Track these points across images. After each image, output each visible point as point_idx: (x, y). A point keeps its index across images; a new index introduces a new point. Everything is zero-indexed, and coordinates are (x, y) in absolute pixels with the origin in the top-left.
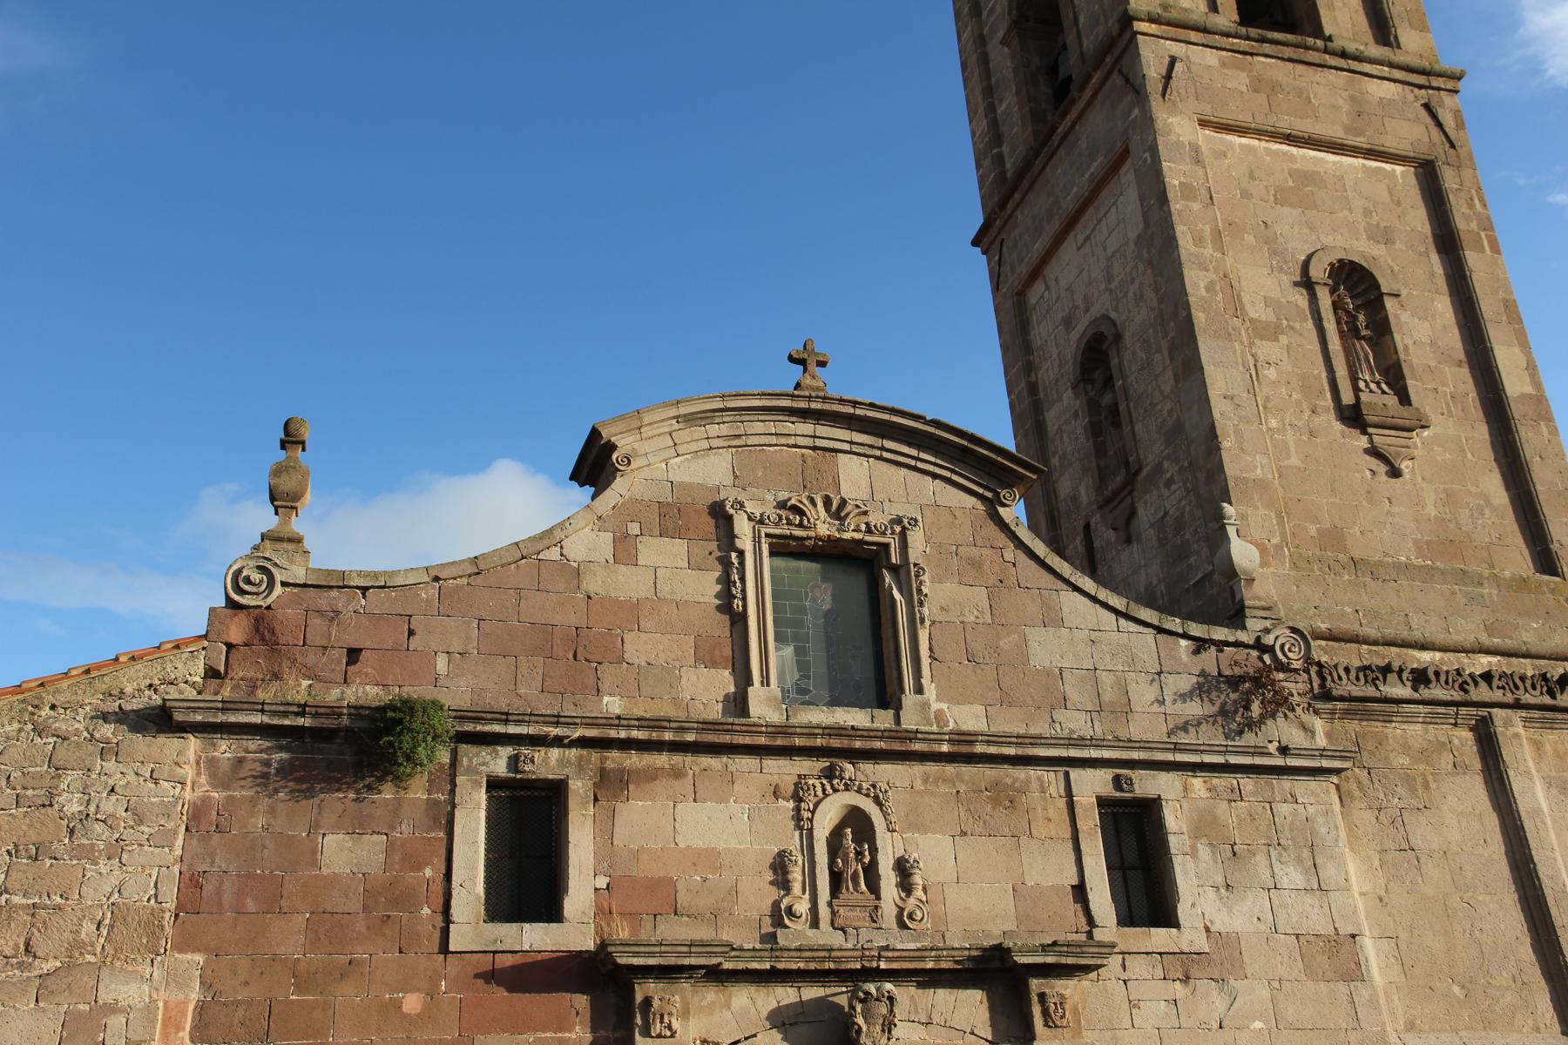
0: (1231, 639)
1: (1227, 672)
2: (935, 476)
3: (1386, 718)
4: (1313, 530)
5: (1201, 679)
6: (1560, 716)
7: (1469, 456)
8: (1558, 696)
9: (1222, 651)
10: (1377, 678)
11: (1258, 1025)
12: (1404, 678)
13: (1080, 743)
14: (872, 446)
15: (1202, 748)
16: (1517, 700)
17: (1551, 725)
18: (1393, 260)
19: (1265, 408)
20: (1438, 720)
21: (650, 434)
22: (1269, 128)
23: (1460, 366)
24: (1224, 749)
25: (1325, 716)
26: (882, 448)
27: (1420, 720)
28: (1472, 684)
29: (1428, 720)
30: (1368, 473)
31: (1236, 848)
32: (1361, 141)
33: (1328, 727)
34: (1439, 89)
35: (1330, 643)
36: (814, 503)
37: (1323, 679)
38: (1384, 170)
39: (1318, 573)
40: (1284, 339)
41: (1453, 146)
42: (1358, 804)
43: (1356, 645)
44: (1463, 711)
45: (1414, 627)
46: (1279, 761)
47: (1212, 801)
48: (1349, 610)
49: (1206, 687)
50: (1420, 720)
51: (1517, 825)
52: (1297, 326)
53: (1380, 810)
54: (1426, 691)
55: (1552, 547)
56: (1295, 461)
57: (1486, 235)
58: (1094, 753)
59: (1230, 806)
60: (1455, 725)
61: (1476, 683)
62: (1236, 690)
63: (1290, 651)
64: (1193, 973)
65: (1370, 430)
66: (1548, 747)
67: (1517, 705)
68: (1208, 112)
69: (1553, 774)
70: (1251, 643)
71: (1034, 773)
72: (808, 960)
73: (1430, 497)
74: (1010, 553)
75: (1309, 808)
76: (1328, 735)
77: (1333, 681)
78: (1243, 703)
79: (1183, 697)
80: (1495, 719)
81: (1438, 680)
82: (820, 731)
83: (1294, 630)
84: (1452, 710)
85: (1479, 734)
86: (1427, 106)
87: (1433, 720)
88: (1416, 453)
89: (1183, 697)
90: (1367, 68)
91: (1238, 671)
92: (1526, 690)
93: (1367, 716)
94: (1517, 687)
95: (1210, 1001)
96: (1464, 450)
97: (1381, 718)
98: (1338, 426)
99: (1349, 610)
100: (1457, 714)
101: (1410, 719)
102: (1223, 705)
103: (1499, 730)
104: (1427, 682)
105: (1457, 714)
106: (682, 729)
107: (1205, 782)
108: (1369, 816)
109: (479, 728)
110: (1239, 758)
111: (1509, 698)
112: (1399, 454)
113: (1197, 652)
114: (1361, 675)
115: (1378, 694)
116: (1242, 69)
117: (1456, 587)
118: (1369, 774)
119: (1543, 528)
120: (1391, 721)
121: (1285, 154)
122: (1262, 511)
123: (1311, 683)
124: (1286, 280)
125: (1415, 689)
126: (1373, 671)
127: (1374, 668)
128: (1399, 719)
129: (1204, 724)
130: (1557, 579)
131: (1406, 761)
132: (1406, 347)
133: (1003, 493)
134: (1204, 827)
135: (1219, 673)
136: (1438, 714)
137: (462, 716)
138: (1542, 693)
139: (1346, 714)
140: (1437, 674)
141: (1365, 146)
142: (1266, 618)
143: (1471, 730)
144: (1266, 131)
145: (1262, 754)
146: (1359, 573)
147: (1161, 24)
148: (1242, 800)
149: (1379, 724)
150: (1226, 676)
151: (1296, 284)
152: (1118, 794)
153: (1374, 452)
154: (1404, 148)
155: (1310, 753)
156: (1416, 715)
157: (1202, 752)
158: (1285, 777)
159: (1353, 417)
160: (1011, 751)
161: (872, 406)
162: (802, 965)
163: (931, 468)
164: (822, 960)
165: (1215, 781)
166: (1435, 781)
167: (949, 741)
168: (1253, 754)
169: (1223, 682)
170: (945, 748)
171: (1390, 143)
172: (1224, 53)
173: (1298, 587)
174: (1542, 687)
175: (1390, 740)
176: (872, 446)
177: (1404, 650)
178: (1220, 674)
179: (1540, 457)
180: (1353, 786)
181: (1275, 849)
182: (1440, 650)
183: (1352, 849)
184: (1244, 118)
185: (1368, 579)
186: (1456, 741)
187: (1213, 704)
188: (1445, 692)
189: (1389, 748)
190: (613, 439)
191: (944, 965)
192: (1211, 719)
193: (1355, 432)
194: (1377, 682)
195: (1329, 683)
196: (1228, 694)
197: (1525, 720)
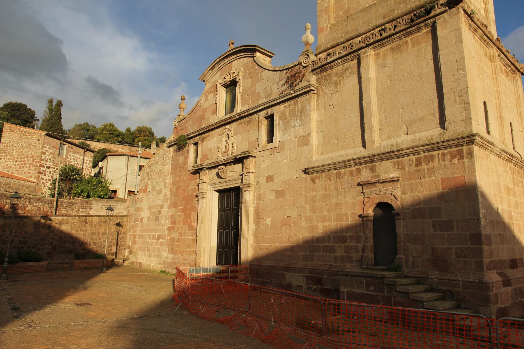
4: (342, 12)
6: (384, 41)
11: (285, 161)
17: (383, 46)
20: (346, 62)
26: (238, 57)
27: (341, 64)
29: (343, 63)
33: (317, 77)
35: (333, 49)
42: (321, 96)
44: (352, 55)
50: (341, 64)
58: (259, 108)
60: (352, 60)
64: (275, 152)
66: (381, 54)
67: (367, 46)
71: (254, 116)
72: (216, 164)
74: (257, 67)
79: (283, 85)
84: (349, 57)
89: (283, 85)
93: (326, 70)
95: (278, 156)
97: (330, 68)
101: (338, 65)
105: (351, 57)
106: (206, 128)
109: (189, 137)
117: (379, 7)
120: (333, 68)
122: (324, 17)
128: (335, 66)
133: (254, 54)
134: (283, 117)
137: (187, 136)
139: (321, 72)
149: (330, 70)
152: (267, 115)
155: (300, 89)
156: (338, 63)
160: (247, 114)
161: (232, 50)
162: (215, 165)
163: (245, 56)
164: (217, 163)
170: (237, 117)
177: (353, 40)
180: (321, 92)
182: (364, 34)
183: (317, 110)
186: (351, 66)
191: (232, 161)
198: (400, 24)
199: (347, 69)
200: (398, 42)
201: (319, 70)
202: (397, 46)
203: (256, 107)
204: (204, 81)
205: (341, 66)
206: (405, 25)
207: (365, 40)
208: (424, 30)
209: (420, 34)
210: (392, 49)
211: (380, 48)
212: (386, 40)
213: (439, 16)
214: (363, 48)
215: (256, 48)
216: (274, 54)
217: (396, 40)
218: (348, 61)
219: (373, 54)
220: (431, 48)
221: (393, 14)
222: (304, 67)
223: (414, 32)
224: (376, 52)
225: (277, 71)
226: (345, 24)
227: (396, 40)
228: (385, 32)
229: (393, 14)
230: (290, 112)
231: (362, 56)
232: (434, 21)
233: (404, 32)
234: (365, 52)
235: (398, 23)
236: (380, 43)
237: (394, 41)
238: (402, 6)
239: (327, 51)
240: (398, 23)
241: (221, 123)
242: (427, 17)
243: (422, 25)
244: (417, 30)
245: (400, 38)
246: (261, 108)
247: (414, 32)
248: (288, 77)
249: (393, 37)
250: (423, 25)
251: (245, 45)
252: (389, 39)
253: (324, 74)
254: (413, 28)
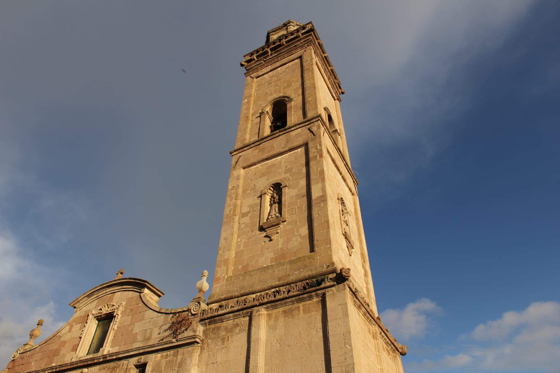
2: (132, 291)
4: (240, 267)
6: (277, 303)
7: (298, 223)
13: (128, 351)
14: (121, 289)
17: (275, 307)
18: (290, 176)
19: (238, 237)
20: (238, 317)
21: (82, 302)
22: (260, 160)
23: (304, 197)
25: (204, 326)
26: (123, 288)
29: (234, 318)
30: (263, 243)
32: (287, 149)
34: (314, 122)
35: (226, 301)
36: (105, 307)
38: (295, 152)
40: (250, 215)
41: (314, 135)
42: (205, 351)
43: (233, 299)
44: (245, 311)
50: (232, 318)
52: (255, 209)
56: (242, 248)
57: (319, 155)
58: (131, 353)
60: (244, 317)
65: (266, 230)
66: (274, 315)
67: (261, 305)
68: (245, 165)
73: (281, 241)
74: (141, 304)
79: (165, 331)
82: (78, 362)
86: (309, 129)
87: (236, 317)
88: (279, 231)
89: (165, 331)
90: (293, 129)
93: (215, 322)
96: (297, 223)
97: (220, 321)
98: (259, 232)
101: (229, 319)
105: (243, 313)
110: (166, 345)
112: (272, 234)
116: (256, 149)
117: (275, 269)
120: (223, 322)
121: (266, 163)
122: (223, 267)
124: (256, 197)
128: (225, 320)
132: (285, 201)
133: (142, 290)
136: (236, 315)
139: (210, 323)
141: (287, 149)
144: (260, 161)
146: (245, 277)
147: (238, 151)
149: (220, 323)
151: (258, 197)
152: (138, 363)
153: (266, 236)
154: (300, 142)
155: (184, 339)
156: (229, 317)
159: (262, 229)
160: (114, 357)
161: (118, 279)
163: (131, 289)
167: (102, 358)
170: (101, 360)
171: (295, 144)
172: (253, 148)
175: (222, 327)
176: (121, 289)
177: (248, 296)
179: (319, 214)
180: (206, 345)
182: (259, 292)
183: (198, 367)
184: (256, 160)
186: (242, 322)
190: (74, 306)
193: (262, 232)
198: (294, 289)
199: (237, 325)
200: (290, 306)
201: (208, 320)
202: (290, 310)
203: (128, 351)
204: (75, 308)
205: (232, 320)
206: (298, 291)
207: (259, 298)
208: (315, 300)
209: (311, 302)
210: (285, 312)
211: (273, 309)
212: (279, 302)
213: (329, 289)
214: (256, 306)
215: (146, 283)
216: (164, 294)
217: (289, 304)
218: (240, 316)
219: (265, 314)
220: (321, 317)
221: (288, 278)
222: (193, 315)
223: (306, 299)
224: (269, 313)
225: (163, 313)
226: (241, 278)
227: (289, 304)
228: (279, 295)
229: (288, 278)
230: (166, 364)
231: (254, 314)
232: (324, 293)
233: (297, 298)
234: (258, 311)
235: (291, 288)
236: (273, 304)
237: (287, 304)
238: (296, 273)
239: (220, 302)
240: (291, 288)
241: (79, 365)
242: (318, 288)
243: (313, 294)
244: (309, 298)
245: (293, 302)
246: (134, 353)
247: (306, 299)
248: (173, 322)
250: (314, 294)
251: (134, 277)
252: (282, 302)
253: (213, 326)
254: (305, 296)
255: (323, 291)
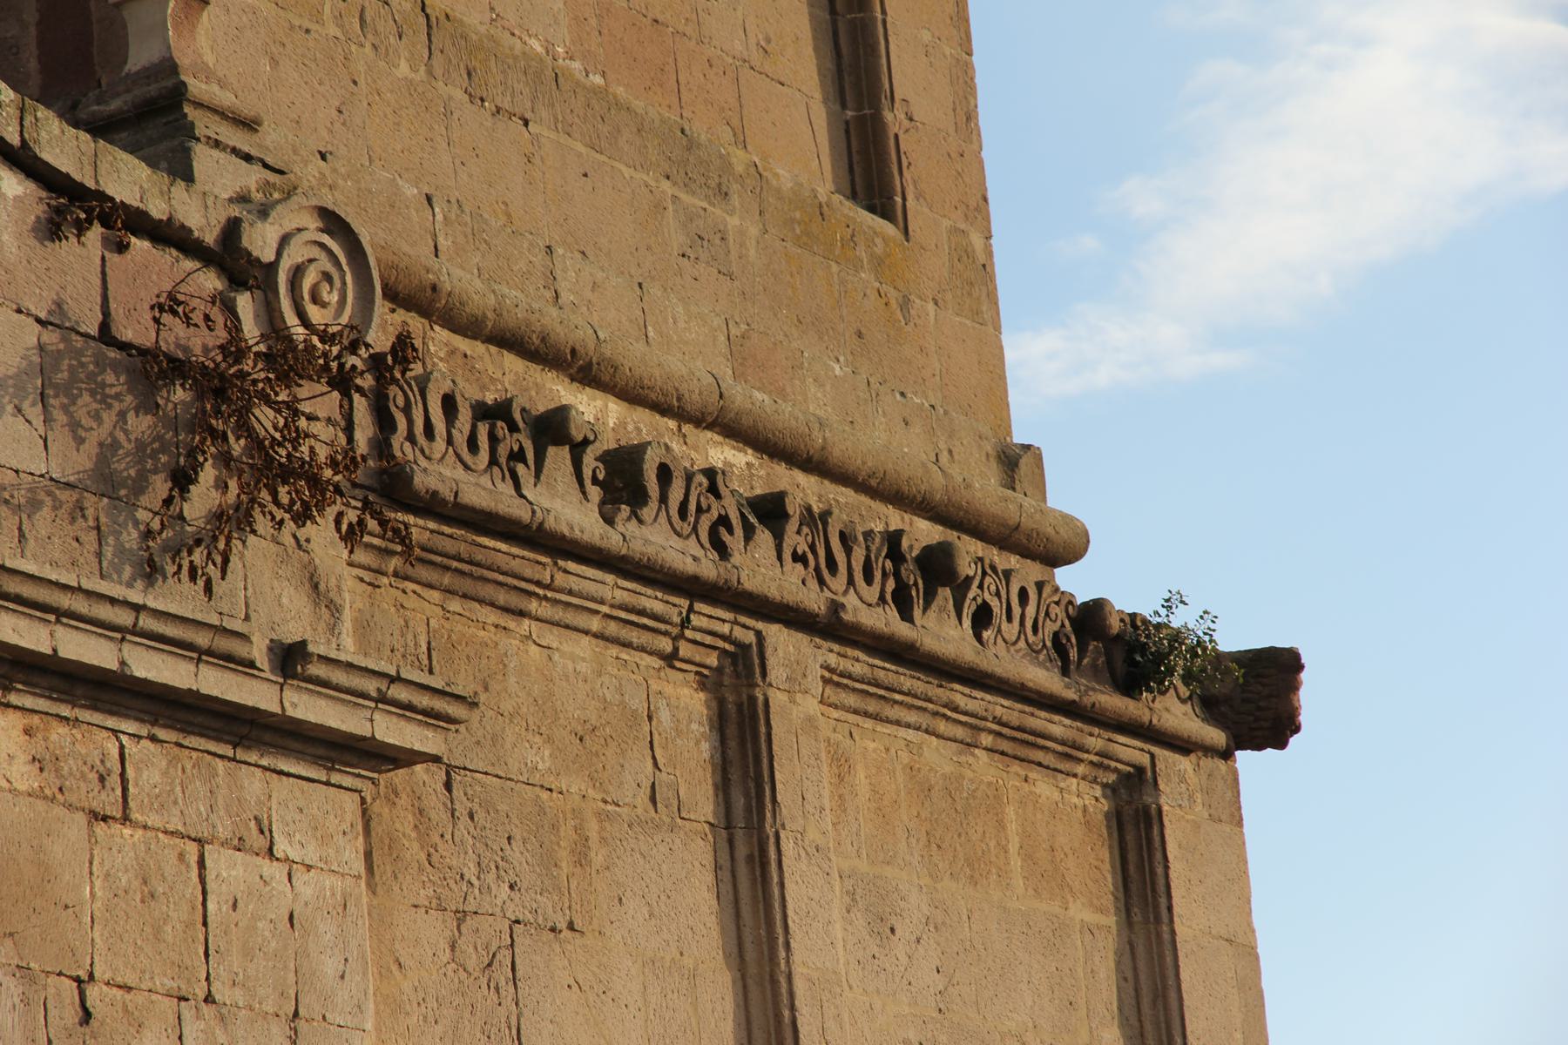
0: (157, 209)
1: (135, 329)
3: (515, 600)
5: (51, 337)
6: (907, 680)
8: (917, 613)
9: (122, 248)
10: (518, 456)
12: (587, 474)
15: (65, 601)
16: (836, 607)
24: (124, 618)
27: (595, 624)
28: (739, 531)
31: (93, 992)
37: (384, 422)
39: (333, 30)
45: (566, 297)
46: (258, 694)
47: (40, 805)
48: (411, 191)
49: (62, 376)
50: (595, 624)
51: (778, 1016)
53: (461, 916)
54: (632, 526)
55: (888, 116)
59: (91, 834)
60: (670, 659)
61: (749, 532)
62: (148, 405)
63: (316, 299)
69: (863, 866)
70: (210, 238)
75: (300, 876)
76: (364, 628)
77: (411, 438)
78: (164, 458)
80: (771, 661)
81: (663, 499)
83: (333, 223)
85: (721, 702)
91: (175, 335)
92: (851, 582)
94: (832, 565)
99: (411, 191)
100: (685, 623)
101: (570, 617)
102: (108, 449)
103: (778, 699)
104: (637, 498)
105: (685, 623)
107: (28, 732)
108: (433, 930)
111: (814, 600)
113: (52, 229)
114: (483, 430)
115: (520, 512)
117: (666, 185)
118: (448, 786)
119: (872, 50)
120: (522, 614)
123: (349, 429)
125: (609, 520)
126: (513, 428)
127: (517, 416)
128: (545, 610)
129: (46, 512)
130: (889, 229)
131: (543, 759)
135: (105, 326)
136: (642, 612)
138: (882, 599)
140: (665, 473)
142: (247, 158)
143: (703, 684)
145: (229, 660)
148: (126, 819)
150: (124, 346)
156: (588, 604)
157: (61, 614)
158: (253, 757)
165: (59, 732)
166: (603, 840)
168: (201, 655)
169: (115, 366)
173: (274, 62)
174: (885, 575)
178: (106, 334)
180: (404, 823)
181: (199, 1016)
185: (459, 94)
186: (664, 715)
187: (80, 441)
188: (675, 542)
189: (507, 706)
192: (64, 495)
194: (520, 469)
195: (398, 440)
196: (122, 415)
197: (834, 678)
232: (1140, 770)
236: (888, 672)
243: (1095, 740)
249: (960, 695)
254: (1059, 726)
255: (1130, 751)
